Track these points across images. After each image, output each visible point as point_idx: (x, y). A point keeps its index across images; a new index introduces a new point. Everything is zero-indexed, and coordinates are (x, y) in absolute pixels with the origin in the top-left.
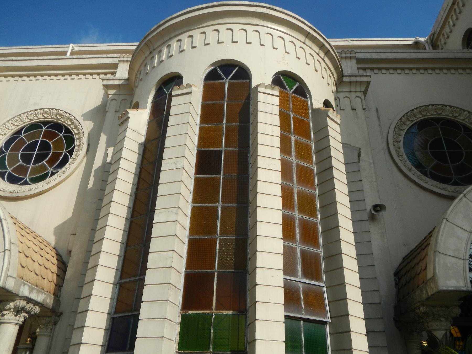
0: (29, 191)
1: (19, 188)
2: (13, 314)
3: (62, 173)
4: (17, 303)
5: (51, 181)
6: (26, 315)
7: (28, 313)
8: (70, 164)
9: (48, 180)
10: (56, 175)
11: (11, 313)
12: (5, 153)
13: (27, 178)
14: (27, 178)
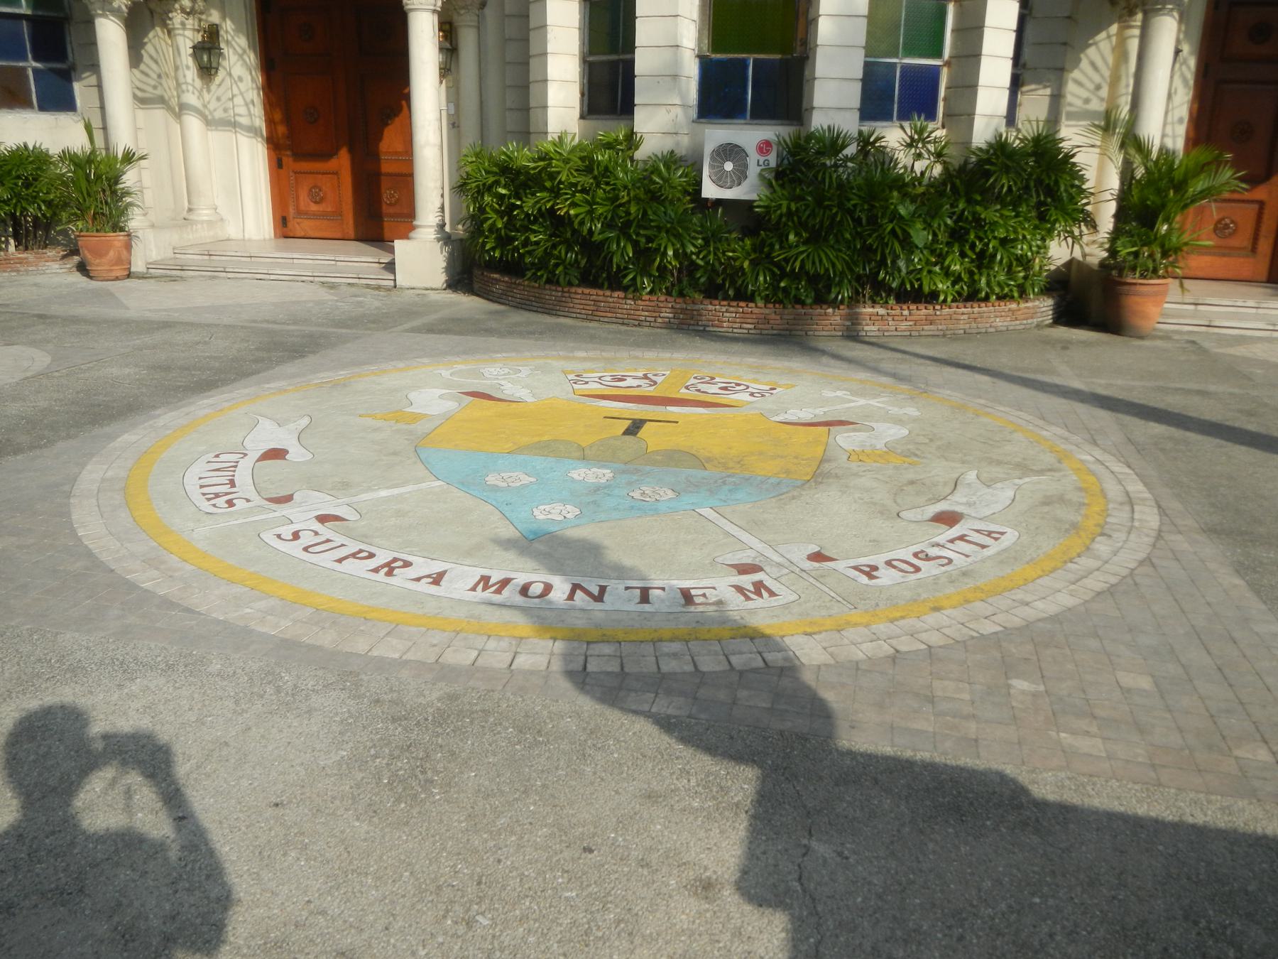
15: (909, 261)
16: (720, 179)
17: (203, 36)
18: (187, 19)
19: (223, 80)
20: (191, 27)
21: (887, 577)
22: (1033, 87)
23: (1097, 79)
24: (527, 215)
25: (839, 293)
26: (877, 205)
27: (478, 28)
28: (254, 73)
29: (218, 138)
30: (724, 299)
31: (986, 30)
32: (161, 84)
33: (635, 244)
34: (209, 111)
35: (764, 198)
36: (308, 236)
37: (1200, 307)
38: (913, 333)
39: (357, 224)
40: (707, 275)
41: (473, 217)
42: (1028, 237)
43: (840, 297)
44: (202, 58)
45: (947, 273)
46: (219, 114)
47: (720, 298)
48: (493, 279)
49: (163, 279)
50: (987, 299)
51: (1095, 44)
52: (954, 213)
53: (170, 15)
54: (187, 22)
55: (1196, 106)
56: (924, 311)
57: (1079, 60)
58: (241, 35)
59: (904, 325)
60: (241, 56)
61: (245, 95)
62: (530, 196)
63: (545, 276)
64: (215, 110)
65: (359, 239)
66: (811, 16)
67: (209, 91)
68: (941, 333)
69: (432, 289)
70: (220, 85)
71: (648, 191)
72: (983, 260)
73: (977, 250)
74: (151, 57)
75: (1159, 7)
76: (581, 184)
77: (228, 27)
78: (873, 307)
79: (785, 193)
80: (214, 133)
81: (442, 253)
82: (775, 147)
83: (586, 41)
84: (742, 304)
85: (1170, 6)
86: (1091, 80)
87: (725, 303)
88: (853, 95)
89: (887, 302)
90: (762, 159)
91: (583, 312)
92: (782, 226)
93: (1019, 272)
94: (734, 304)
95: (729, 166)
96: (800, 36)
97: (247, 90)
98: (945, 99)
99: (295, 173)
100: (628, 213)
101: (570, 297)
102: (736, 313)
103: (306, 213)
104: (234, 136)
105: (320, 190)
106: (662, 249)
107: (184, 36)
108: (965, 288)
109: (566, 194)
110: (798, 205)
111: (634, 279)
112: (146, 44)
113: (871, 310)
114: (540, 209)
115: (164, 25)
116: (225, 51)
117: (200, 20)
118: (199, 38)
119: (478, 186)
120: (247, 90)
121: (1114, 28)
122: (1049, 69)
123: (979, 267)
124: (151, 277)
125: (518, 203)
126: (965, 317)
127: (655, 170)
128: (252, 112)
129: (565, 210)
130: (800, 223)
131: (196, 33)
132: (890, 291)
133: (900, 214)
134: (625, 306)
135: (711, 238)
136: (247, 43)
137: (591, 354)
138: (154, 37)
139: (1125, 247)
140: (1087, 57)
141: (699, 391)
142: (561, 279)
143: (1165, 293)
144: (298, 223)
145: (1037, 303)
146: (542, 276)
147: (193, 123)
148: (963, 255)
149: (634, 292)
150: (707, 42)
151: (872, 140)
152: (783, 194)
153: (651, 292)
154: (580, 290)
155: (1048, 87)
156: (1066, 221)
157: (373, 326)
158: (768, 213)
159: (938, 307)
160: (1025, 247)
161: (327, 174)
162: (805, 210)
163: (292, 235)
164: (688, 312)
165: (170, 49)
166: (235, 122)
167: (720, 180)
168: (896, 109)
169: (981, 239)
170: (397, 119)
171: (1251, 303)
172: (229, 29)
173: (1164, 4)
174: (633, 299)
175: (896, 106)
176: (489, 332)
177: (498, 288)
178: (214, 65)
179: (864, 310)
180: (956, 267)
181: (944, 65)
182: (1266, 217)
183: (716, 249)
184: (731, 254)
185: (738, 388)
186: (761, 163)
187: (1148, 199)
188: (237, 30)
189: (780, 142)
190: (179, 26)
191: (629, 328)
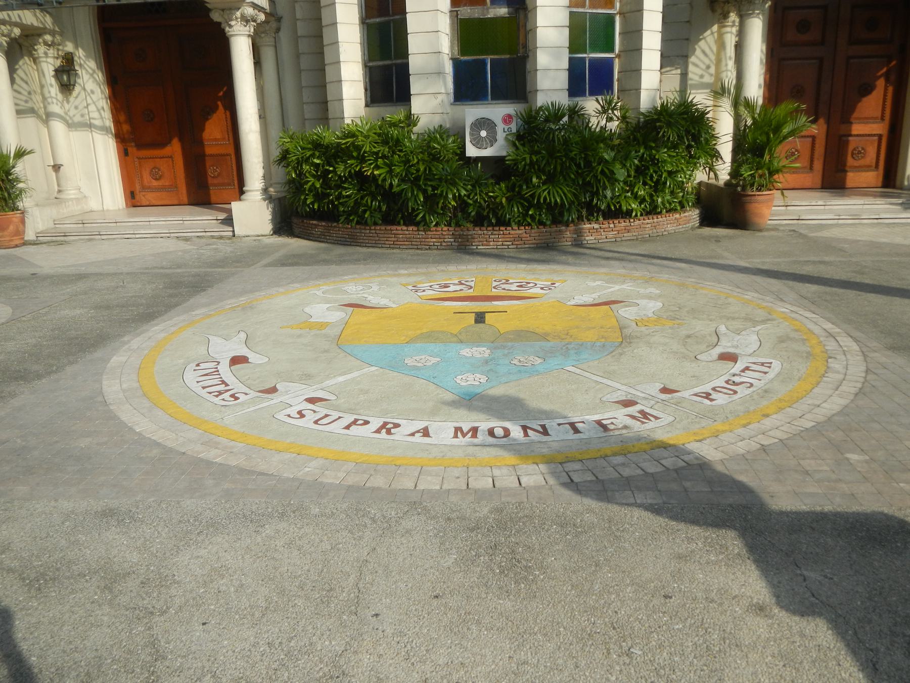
4: (243, 10)
6: (255, 24)
15: (613, 190)
16: (478, 143)
17: (62, 62)
19: (79, 94)
20: (52, 55)
21: (720, 399)
22: (668, 69)
23: (707, 61)
24: (340, 177)
25: (569, 216)
26: (590, 154)
27: (276, 47)
28: (102, 87)
29: (78, 136)
30: (488, 226)
31: (644, 32)
32: (31, 99)
33: (424, 192)
34: (70, 116)
35: (512, 154)
36: (152, 204)
37: (789, 208)
38: (618, 239)
39: (189, 193)
40: (475, 211)
41: (291, 182)
42: (685, 169)
43: (570, 219)
44: (63, 78)
45: (636, 196)
46: (77, 119)
47: (485, 225)
48: (312, 224)
49: (52, 244)
50: (660, 213)
51: (704, 38)
52: (637, 156)
53: (36, 47)
54: (48, 51)
55: (768, 76)
56: (623, 223)
57: (695, 50)
58: (90, 60)
59: (611, 234)
60: (92, 75)
61: (97, 103)
62: (341, 164)
63: (356, 219)
64: (74, 116)
65: (191, 204)
66: (529, 27)
67: (68, 102)
68: (635, 238)
69: (262, 236)
71: (430, 154)
72: (658, 187)
73: (655, 180)
74: (22, 79)
75: (751, 12)
76: (382, 151)
77: (80, 54)
78: (590, 223)
79: (526, 149)
80: (74, 133)
81: (268, 209)
82: (514, 119)
83: (366, 52)
84: (502, 228)
85: (758, 12)
86: (704, 63)
87: (490, 228)
88: (562, 80)
89: (597, 220)
90: (506, 128)
91: (387, 242)
92: (526, 172)
93: (679, 193)
94: (497, 228)
95: (483, 133)
96: (521, 42)
97: (99, 100)
98: (618, 80)
99: (139, 158)
100: (418, 171)
101: (376, 233)
102: (499, 235)
103: (149, 188)
104: (90, 134)
105: (159, 170)
106: (444, 194)
107: (47, 62)
108: (648, 206)
109: (370, 160)
110: (538, 157)
111: (424, 217)
112: (17, 69)
113: (589, 226)
114: (350, 172)
115: (31, 55)
116: (79, 72)
117: (58, 50)
118: (58, 63)
119: (298, 159)
120: (99, 100)
121: (715, 28)
122: (678, 56)
123: (656, 191)
124: (41, 243)
125: (331, 169)
126: (649, 225)
127: (434, 139)
128: (103, 116)
129: (370, 171)
130: (539, 169)
131: (56, 60)
132: (599, 210)
133: (605, 159)
134: (418, 236)
135: (476, 183)
137: (411, 271)
138: (24, 64)
139: (746, 171)
140: (700, 47)
141: (504, 289)
142: (369, 221)
143: (772, 200)
144: (144, 196)
145: (690, 213)
146: (353, 219)
147: (58, 126)
148: (645, 184)
149: (424, 225)
150: (457, 48)
151: (576, 109)
152: (524, 151)
153: (436, 225)
154: (383, 228)
155: (679, 68)
156: (705, 156)
157: (238, 264)
158: (515, 164)
159: (632, 220)
160: (682, 176)
161: (163, 157)
162: (542, 161)
163: (139, 204)
164: (464, 237)
165: (36, 73)
166: (90, 124)
167: (478, 143)
168: (587, 89)
169: (655, 172)
170: (215, 115)
171: (820, 203)
172: (81, 55)
173: (754, 10)
174: (424, 231)
175: (587, 86)
176: (326, 262)
177: (318, 231)
178: (72, 83)
179: (585, 226)
180: (641, 193)
181: (616, 57)
182: (817, 146)
183: (481, 191)
184: (492, 194)
185: (529, 285)
186: (506, 130)
187: (758, 139)
188: (87, 57)
189: (517, 114)
191: (423, 251)
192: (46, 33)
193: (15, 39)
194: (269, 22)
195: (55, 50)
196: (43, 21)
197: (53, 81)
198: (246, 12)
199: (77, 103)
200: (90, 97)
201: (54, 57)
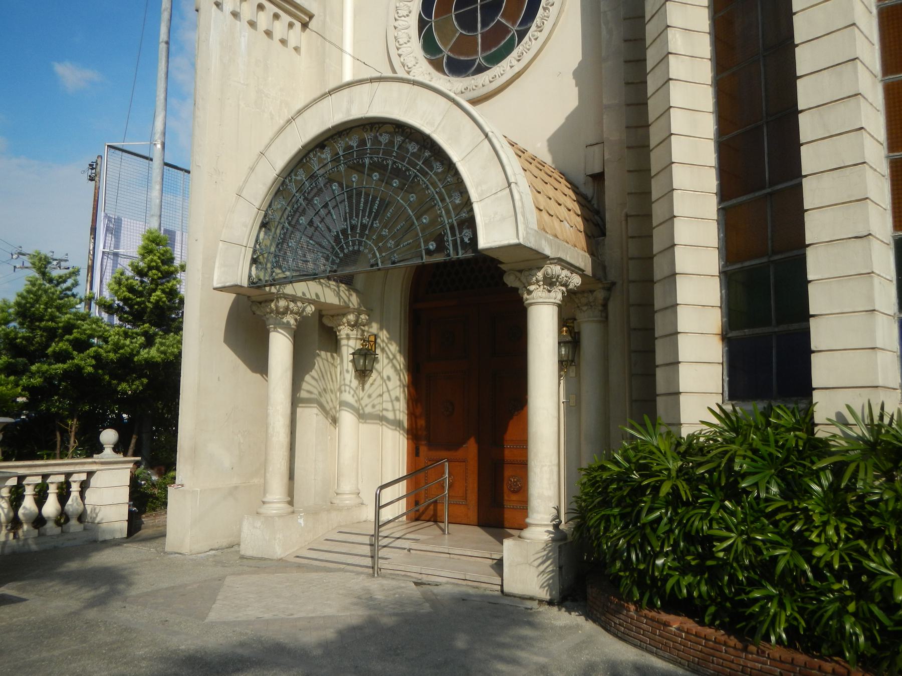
0: (491, 82)
1: (473, 82)
2: (544, 288)
3: (536, 31)
5: (523, 54)
6: (564, 289)
7: (565, 285)
8: (545, 9)
9: (515, 53)
10: (526, 39)
11: (542, 287)
12: (429, 22)
13: (480, 58)
14: (480, 58)
18: (352, 330)
20: (355, 337)
46: (368, 410)
58: (393, 343)
61: (391, 393)
67: (363, 389)
70: (372, 384)
117: (363, 331)
136: (398, 348)
147: (347, 418)
188: (390, 339)
190: (345, 336)
192: (349, 313)
193: (307, 317)
194: (594, 291)
195: (360, 331)
196: (346, 299)
197: (350, 367)
198: (549, 271)
199: (370, 391)
200: (386, 384)
201: (357, 339)
